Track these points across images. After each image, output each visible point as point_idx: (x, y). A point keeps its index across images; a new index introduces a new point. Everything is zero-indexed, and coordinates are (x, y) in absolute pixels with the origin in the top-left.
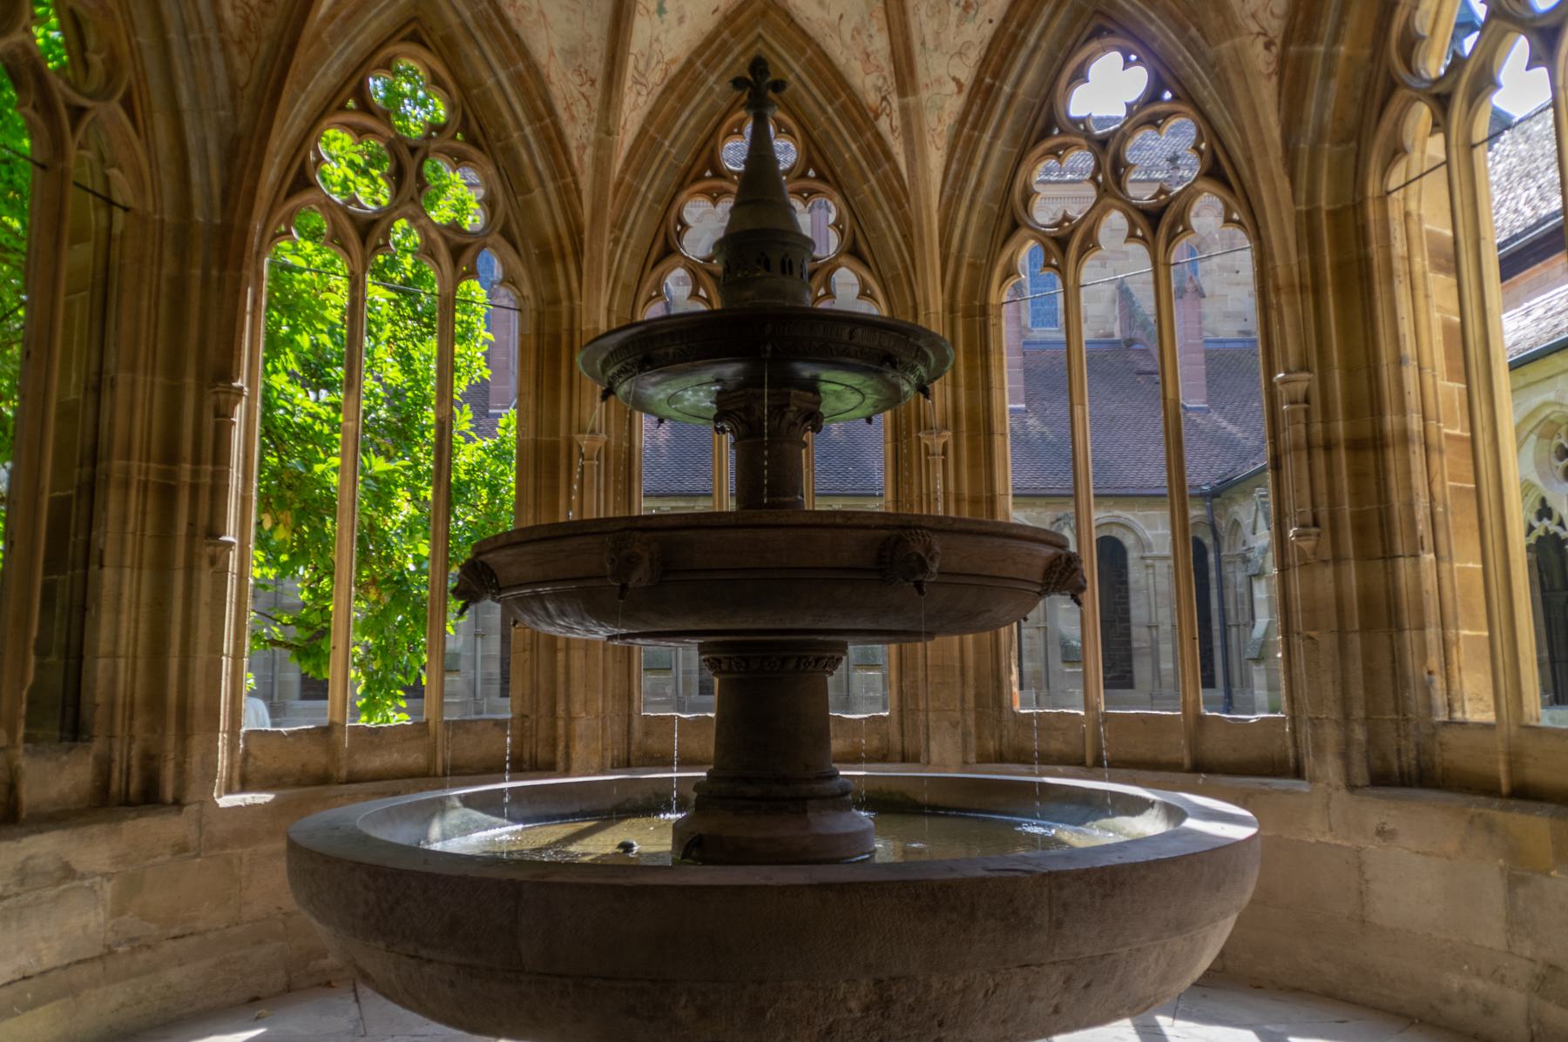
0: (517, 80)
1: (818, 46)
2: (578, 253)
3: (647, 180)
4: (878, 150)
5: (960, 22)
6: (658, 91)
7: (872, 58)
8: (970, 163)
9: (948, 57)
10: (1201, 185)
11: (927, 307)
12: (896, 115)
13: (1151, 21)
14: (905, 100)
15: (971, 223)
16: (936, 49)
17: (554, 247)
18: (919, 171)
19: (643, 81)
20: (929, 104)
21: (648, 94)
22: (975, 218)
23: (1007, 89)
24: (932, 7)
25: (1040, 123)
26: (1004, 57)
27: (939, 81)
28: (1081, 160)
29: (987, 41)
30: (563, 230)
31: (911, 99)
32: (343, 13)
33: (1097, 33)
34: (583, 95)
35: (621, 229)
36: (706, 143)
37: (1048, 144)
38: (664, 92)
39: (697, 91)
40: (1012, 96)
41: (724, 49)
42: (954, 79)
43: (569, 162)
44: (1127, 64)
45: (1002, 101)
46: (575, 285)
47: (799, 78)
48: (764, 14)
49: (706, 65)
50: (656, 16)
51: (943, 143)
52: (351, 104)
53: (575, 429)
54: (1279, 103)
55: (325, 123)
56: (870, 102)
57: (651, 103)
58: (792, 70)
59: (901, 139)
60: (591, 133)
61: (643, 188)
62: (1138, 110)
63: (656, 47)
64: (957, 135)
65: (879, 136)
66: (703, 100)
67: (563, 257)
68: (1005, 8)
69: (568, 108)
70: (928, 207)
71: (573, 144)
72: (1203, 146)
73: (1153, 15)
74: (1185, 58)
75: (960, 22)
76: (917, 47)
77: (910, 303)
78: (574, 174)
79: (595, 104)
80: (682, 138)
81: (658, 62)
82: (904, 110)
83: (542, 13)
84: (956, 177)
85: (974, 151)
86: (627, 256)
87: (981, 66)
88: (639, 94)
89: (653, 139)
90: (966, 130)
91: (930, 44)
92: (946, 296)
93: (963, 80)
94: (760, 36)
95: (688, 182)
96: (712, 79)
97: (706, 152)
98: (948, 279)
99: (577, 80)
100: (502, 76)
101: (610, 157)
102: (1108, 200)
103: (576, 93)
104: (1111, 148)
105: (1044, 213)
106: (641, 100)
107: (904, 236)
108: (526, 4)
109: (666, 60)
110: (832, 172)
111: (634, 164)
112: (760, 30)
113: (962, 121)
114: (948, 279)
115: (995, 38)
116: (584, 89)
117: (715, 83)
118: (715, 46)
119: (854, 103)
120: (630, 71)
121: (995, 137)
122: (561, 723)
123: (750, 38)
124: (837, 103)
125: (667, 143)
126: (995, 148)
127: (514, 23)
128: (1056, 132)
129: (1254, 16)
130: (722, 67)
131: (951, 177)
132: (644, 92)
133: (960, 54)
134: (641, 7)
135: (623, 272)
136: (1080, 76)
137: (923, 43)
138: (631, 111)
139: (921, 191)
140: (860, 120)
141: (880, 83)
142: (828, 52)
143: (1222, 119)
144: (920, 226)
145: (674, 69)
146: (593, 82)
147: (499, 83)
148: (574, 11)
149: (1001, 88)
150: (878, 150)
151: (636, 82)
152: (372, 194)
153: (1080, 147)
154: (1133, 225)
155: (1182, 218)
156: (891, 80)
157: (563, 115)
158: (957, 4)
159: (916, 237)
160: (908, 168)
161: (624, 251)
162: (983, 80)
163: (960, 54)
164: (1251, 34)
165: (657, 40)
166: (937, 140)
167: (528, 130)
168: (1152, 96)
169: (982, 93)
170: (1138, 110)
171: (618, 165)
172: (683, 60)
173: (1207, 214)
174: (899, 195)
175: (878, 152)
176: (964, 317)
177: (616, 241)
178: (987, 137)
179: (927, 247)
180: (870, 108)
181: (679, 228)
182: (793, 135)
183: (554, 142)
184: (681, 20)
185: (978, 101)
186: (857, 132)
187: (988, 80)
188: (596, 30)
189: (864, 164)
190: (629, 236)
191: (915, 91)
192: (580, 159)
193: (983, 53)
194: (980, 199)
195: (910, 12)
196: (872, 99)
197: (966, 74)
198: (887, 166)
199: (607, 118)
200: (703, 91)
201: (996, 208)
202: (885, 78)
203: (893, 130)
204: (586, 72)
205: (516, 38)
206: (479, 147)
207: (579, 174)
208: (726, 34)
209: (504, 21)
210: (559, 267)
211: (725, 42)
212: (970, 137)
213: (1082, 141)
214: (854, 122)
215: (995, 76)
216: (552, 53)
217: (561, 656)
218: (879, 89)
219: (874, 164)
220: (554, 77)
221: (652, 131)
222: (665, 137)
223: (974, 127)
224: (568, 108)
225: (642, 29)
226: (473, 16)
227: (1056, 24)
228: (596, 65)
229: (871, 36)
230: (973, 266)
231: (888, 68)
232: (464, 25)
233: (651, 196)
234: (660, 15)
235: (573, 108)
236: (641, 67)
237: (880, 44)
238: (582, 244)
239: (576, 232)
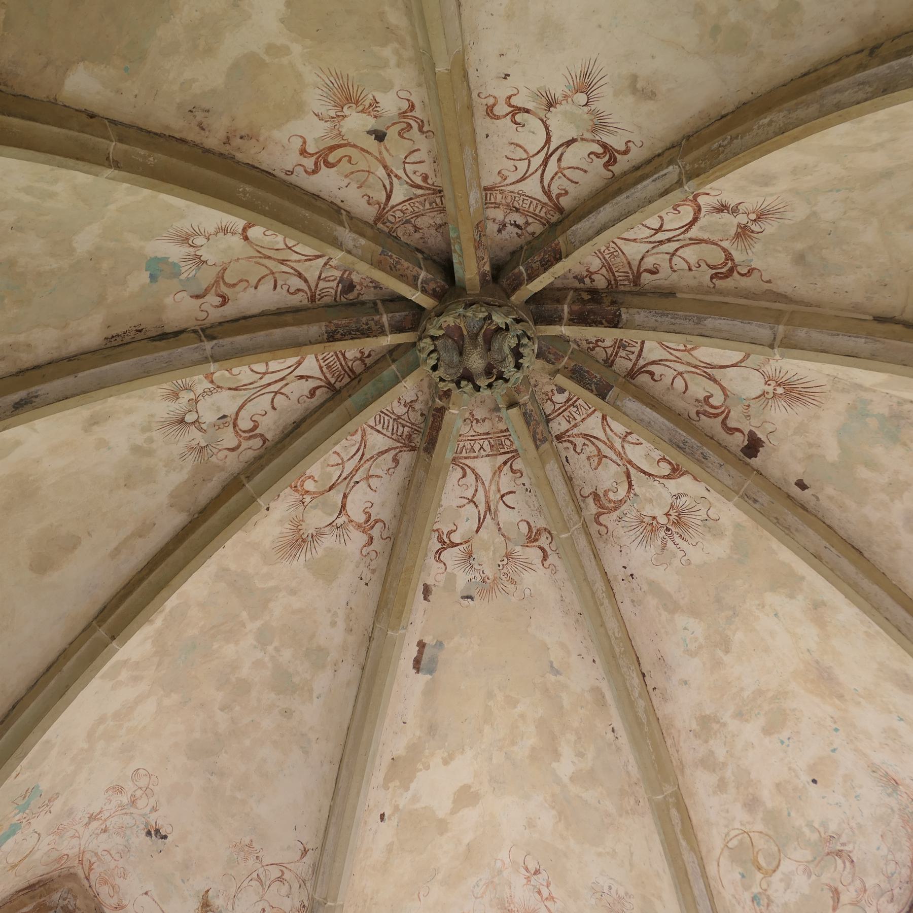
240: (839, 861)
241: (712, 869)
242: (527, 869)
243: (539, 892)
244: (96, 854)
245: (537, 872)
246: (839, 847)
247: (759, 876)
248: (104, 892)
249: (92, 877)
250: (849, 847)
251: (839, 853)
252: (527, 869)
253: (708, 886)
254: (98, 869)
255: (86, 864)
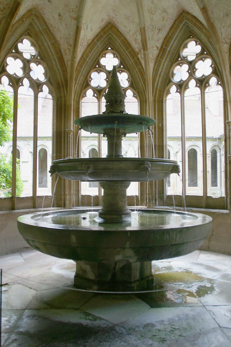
0: (53, 44)
1: (124, 36)
2: (67, 86)
3: (83, 68)
4: (138, 62)
5: (158, 33)
6: (86, 47)
7: (137, 41)
8: (160, 66)
9: (155, 41)
10: (212, 75)
11: (149, 101)
12: (142, 54)
13: (202, 36)
14: (145, 52)
15: (159, 80)
16: (152, 39)
17: (61, 84)
18: (148, 69)
19: (82, 45)
20: (150, 52)
21: (83, 48)
22: (160, 80)
23: (168, 49)
24: (151, 30)
25: (176, 57)
26: (168, 42)
27: (153, 47)
28: (186, 67)
29: (164, 38)
30: (63, 81)
31: (146, 52)
32: (13, 30)
33: (189, 37)
34: (68, 48)
35: (77, 80)
36: (97, 59)
37: (178, 62)
38: (87, 47)
39: (95, 47)
40: (170, 51)
41: (101, 37)
42: (156, 46)
43: (65, 65)
44: (196, 44)
45: (167, 52)
46: (66, 94)
47: (119, 43)
48: (111, 28)
49: (97, 40)
50: (86, 30)
51: (153, 62)
52: (14, 51)
53: (66, 128)
54: (229, 59)
55: (8, 56)
56: (136, 51)
57: (84, 50)
58: (118, 42)
59: (143, 60)
60: (70, 57)
61: (82, 70)
62: (199, 56)
63: (86, 37)
64: (157, 60)
65: (138, 59)
66: (96, 49)
67: (63, 87)
68: (168, 30)
69: (65, 51)
70: (149, 76)
71: (65, 60)
72: (213, 66)
73: (202, 34)
74: (209, 45)
75: (158, 33)
76: (148, 39)
77: (145, 99)
78: (66, 67)
79: (71, 51)
80: (91, 58)
81: (86, 40)
82: (144, 54)
83: (58, 29)
84: (156, 70)
85: (161, 64)
86: (78, 87)
87: (163, 43)
88: (81, 48)
89: (84, 59)
90: (159, 59)
91: (151, 38)
92: (153, 98)
93: (158, 47)
94: (110, 33)
95: (92, 68)
96: (99, 44)
97: (97, 61)
98: (154, 94)
99: (67, 45)
100: (49, 44)
101: (75, 64)
102: (191, 77)
103: (66, 48)
104: (193, 64)
105: (176, 79)
106: (82, 49)
107: (144, 83)
108: (55, 26)
109: (88, 39)
110: (127, 67)
111: (80, 65)
112: (110, 32)
113: (158, 56)
114: (154, 94)
115: (166, 37)
116: (68, 47)
117: (99, 44)
118: (99, 36)
119: (132, 51)
120: (80, 43)
121: (166, 60)
122: (63, 197)
123: (107, 34)
124: (129, 50)
125: (88, 59)
126: (165, 63)
127: (52, 31)
128: (180, 59)
129: (224, 39)
130: (101, 41)
131: (155, 69)
132: (83, 47)
133: (158, 40)
134: (82, 28)
135: (77, 90)
136: (186, 46)
137: (149, 38)
138: (80, 52)
139: (148, 73)
140: (134, 55)
141: (139, 47)
142: (126, 38)
143: (217, 60)
144: (148, 82)
145: (90, 42)
146: (71, 46)
147: (48, 45)
148: (67, 29)
149: (167, 49)
150: (138, 62)
151: (81, 45)
152: (20, 73)
153: (185, 64)
154: (197, 84)
155: (208, 82)
156: (141, 46)
157: (63, 53)
158: (157, 29)
159: (147, 84)
160: (145, 67)
161: (77, 85)
162: (163, 46)
163: (158, 40)
164: (223, 43)
165: (86, 35)
166: (152, 61)
167: (55, 56)
168: (202, 53)
169: (162, 50)
170: (199, 56)
171: (76, 65)
172: (91, 40)
173: (213, 80)
174: (143, 73)
175: (138, 62)
176: (157, 103)
177: (75, 83)
178: (163, 60)
179: (149, 86)
180: (136, 52)
181: (90, 79)
182: (118, 58)
183: (61, 59)
184: (92, 30)
185: (162, 52)
186: (133, 57)
187: (164, 47)
188: (72, 33)
189: (135, 65)
190: (78, 82)
191: (147, 50)
192: (67, 63)
193: (163, 40)
194: (162, 74)
195: (146, 31)
196: (137, 50)
197: (159, 46)
198: (140, 66)
199: (74, 55)
200: (96, 46)
201: (165, 77)
202: (140, 46)
203: (142, 58)
204: (69, 43)
205: (52, 34)
206: (43, 61)
207: (67, 67)
208: (102, 33)
209: (49, 30)
210: (62, 89)
211: (102, 35)
212: (160, 60)
213: (186, 62)
214: (132, 55)
215: (166, 46)
216: (61, 38)
217: (63, 181)
218: (139, 48)
219: (137, 66)
220: (61, 44)
221: (84, 56)
222: (87, 58)
223: (161, 58)
224: (65, 51)
225: (82, 33)
226: (42, 29)
227: (180, 34)
228: (72, 42)
229: (137, 36)
230: (160, 91)
231: (141, 44)
232: (40, 31)
233: (84, 72)
234: (87, 29)
235: (66, 51)
236: (82, 42)
237: (139, 38)
238: (67, 84)
239: (66, 81)
240: (165, 13)
241: (144, 14)
242: (113, 10)
243: (115, 14)
244: (39, 4)
245: (115, 10)
246: (165, 10)
247: (152, 15)
248: (41, 11)
249: (39, 8)
250: (167, 10)
251: (165, 12)
252: (113, 10)
253: (144, 17)
254: (40, 7)
255: (38, 6)
